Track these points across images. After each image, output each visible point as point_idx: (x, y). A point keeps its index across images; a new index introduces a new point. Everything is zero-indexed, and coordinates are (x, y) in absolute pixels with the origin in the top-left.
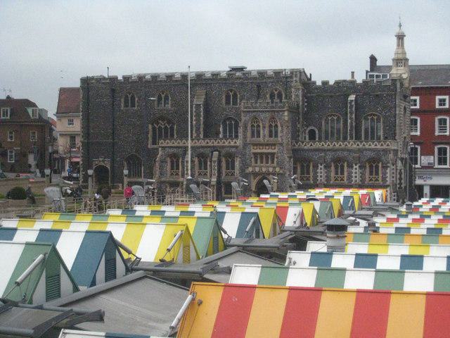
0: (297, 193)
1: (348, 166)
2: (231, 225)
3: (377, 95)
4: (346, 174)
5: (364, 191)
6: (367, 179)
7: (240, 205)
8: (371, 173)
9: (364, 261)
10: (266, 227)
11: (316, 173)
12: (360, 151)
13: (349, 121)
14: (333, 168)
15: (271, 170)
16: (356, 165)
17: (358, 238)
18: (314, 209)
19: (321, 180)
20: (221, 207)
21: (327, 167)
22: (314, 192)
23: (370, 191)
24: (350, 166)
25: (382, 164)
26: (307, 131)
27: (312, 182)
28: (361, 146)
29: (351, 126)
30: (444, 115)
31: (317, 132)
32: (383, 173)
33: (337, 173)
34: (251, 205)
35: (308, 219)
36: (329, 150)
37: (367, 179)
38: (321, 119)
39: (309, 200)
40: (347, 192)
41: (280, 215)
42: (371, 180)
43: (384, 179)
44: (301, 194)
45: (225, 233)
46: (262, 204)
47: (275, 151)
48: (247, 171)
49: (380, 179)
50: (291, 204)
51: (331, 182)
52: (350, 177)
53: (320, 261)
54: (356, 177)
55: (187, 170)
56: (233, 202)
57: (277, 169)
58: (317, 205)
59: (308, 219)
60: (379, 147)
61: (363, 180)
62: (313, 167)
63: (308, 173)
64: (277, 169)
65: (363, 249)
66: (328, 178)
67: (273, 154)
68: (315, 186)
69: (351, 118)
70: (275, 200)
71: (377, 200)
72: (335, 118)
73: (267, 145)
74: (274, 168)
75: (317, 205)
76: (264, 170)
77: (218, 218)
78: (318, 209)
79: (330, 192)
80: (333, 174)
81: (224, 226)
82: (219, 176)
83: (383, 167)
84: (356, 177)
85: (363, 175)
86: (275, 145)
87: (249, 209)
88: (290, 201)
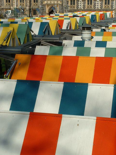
0: (68, 14)
2: (36, 30)
4: (93, 4)
5: (102, 13)
6: (104, 7)
7: (40, 19)
8: (106, 4)
9: (100, 44)
10: (53, 29)
11: (78, 4)
17: (97, 34)
18: (76, 21)
19: (80, 8)
20: (30, 20)
22: (76, 13)
23: (105, 12)
27: (76, 9)
32: (111, 3)
33: (88, 4)
34: (47, 19)
35: (73, 27)
37: (104, 7)
39: (74, 16)
40: (93, 13)
41: (60, 23)
43: (112, 7)
44: (70, 14)
45: (33, 32)
46: (51, 18)
48: (44, 3)
49: (110, 6)
50: (65, 19)
51: (85, 9)
52: (95, 6)
53: (79, 44)
54: (98, 6)
55: (14, 2)
56: (37, 18)
58: (78, 19)
59: (73, 27)
61: (101, 7)
63: (74, 4)
64: (59, 2)
65: (100, 38)
66: (84, 6)
68: (78, 10)
70: (57, 17)
71: (108, 17)
75: (78, 19)
77: (30, 24)
78: (78, 20)
79: (85, 13)
80: (86, 4)
81: (32, 29)
82: (30, 6)
84: (98, 6)
85: (101, 4)
87: (44, 21)
88: (65, 17)
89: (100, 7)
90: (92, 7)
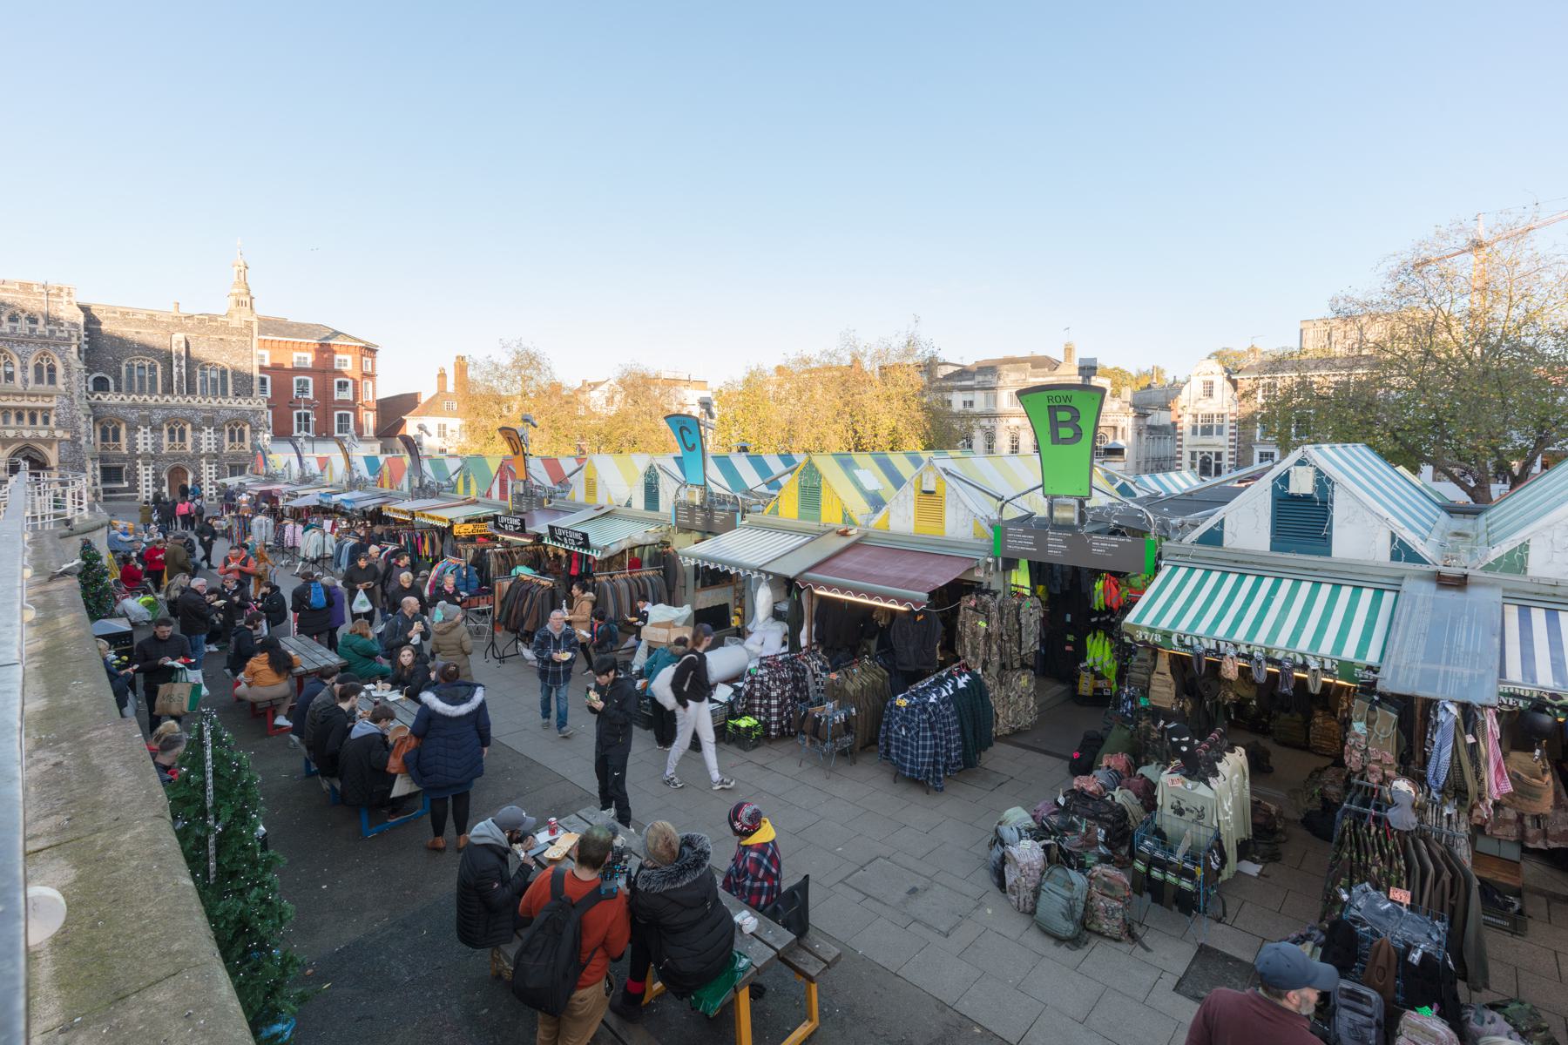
1: (193, 429)
3: (221, 339)
8: (232, 439)
12: (213, 410)
13: (175, 370)
14: (165, 432)
15: (43, 434)
16: (209, 428)
21: (156, 429)
24: (197, 429)
25: (251, 427)
26: (91, 379)
28: (215, 403)
29: (180, 377)
30: (307, 375)
31: (111, 381)
32: (252, 439)
33: (172, 439)
36: (156, 407)
38: (120, 363)
42: (172, 448)
47: (54, 404)
51: (163, 452)
52: (197, 443)
57: (59, 434)
60: (245, 405)
62: (128, 429)
67: (49, 409)
69: (179, 366)
72: (147, 363)
73: (36, 395)
74: (52, 430)
76: (27, 434)
83: (252, 431)
86: (51, 396)
89: (216, 449)
90: (189, 448)
